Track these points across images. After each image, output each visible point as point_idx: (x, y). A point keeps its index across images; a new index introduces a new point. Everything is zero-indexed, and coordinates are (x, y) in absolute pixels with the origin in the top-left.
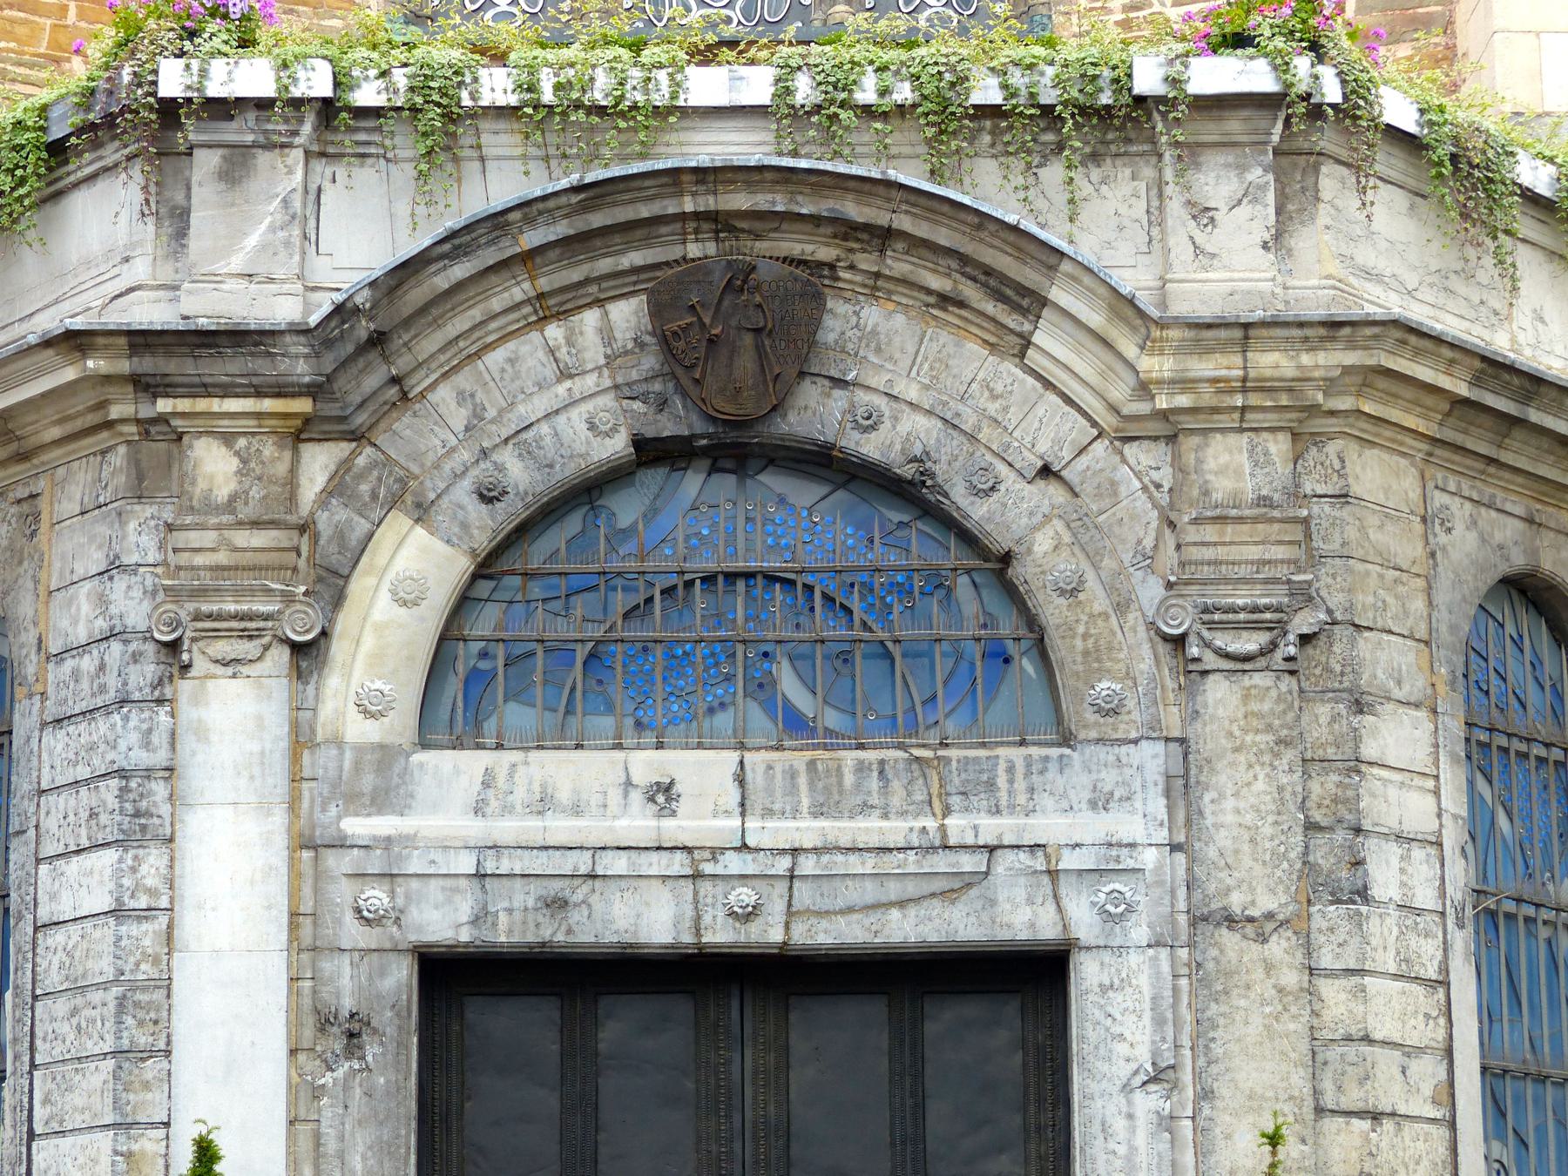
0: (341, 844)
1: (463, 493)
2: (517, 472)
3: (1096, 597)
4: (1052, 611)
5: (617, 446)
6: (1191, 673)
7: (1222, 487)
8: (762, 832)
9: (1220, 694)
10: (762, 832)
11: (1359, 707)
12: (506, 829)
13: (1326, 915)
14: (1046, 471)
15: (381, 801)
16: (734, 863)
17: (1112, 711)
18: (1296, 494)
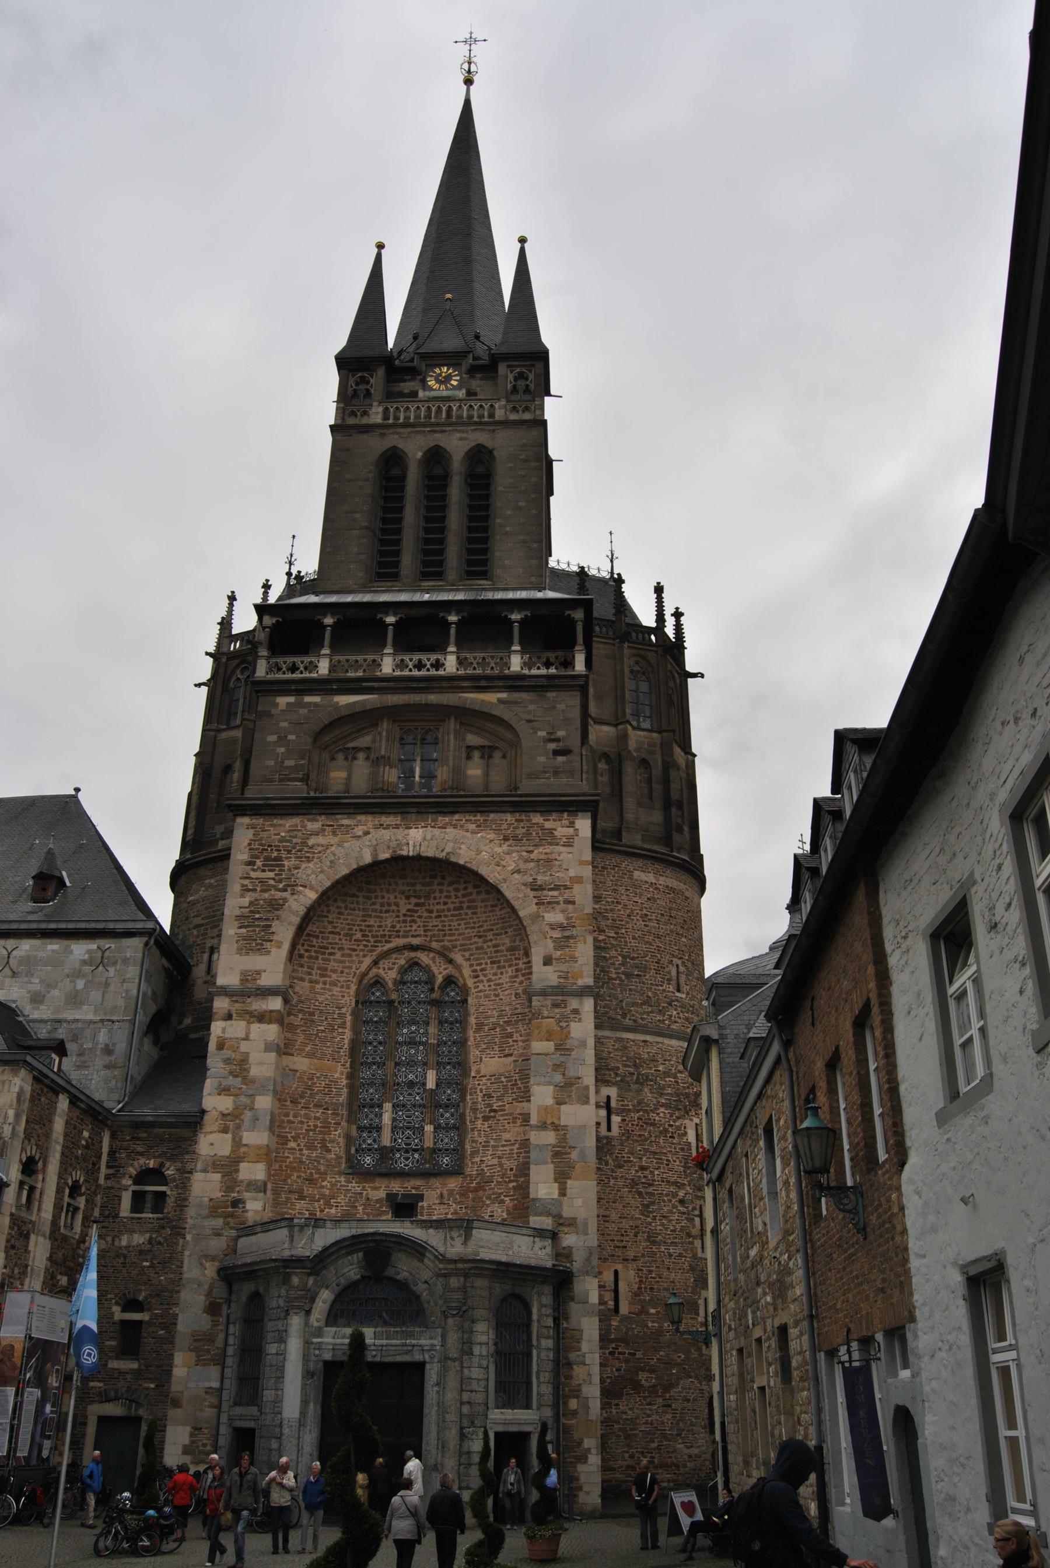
0: (312, 1343)
1: (334, 1284)
2: (342, 1281)
3: (432, 1303)
4: (426, 1306)
5: (358, 1277)
6: (446, 1317)
7: (452, 1286)
8: (378, 1342)
9: (450, 1321)
10: (378, 1342)
11: (473, 1322)
12: (338, 1341)
13: (465, 1357)
14: (426, 1282)
15: (319, 1336)
16: (373, 1348)
17: (434, 1323)
18: (465, 1287)
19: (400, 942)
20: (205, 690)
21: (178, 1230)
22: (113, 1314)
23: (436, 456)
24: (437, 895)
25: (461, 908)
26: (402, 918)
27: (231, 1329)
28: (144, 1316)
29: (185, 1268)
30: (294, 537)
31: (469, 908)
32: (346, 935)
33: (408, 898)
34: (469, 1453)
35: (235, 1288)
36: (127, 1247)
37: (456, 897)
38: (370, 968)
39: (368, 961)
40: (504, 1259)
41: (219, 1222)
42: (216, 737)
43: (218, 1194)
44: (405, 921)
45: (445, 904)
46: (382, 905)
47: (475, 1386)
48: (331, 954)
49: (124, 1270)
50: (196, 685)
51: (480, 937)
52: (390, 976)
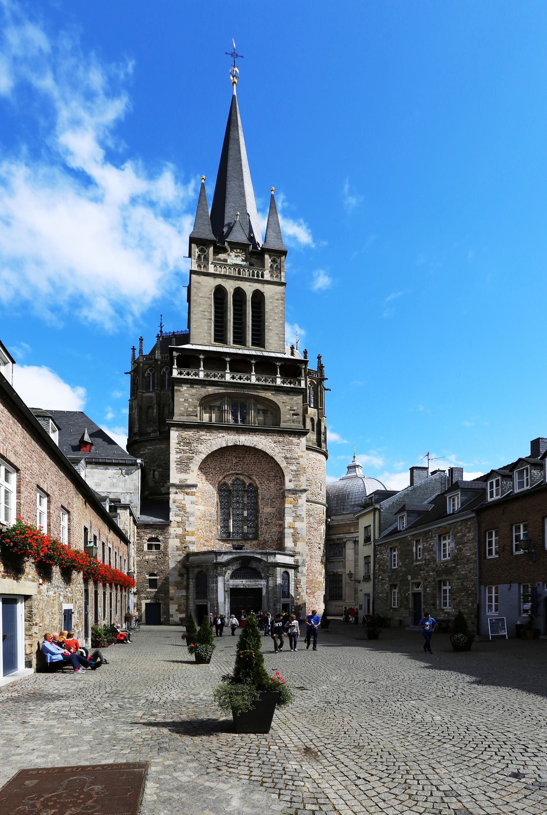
19: (233, 472)
20: (129, 376)
21: (165, 554)
22: (146, 577)
23: (238, 292)
24: (247, 458)
25: (256, 463)
26: (233, 464)
27: (191, 580)
28: (158, 578)
29: (170, 565)
30: (161, 315)
31: (258, 463)
32: (213, 469)
33: (236, 458)
34: (276, 609)
35: (191, 570)
36: (148, 559)
37: (254, 459)
38: (222, 479)
39: (221, 477)
40: (283, 562)
41: (181, 552)
42: (142, 395)
43: (179, 545)
44: (234, 466)
45: (250, 461)
46: (227, 460)
47: (277, 593)
48: (208, 475)
49: (148, 566)
50: (125, 373)
51: (262, 472)
52: (230, 482)
